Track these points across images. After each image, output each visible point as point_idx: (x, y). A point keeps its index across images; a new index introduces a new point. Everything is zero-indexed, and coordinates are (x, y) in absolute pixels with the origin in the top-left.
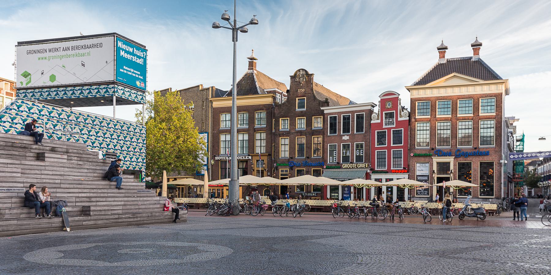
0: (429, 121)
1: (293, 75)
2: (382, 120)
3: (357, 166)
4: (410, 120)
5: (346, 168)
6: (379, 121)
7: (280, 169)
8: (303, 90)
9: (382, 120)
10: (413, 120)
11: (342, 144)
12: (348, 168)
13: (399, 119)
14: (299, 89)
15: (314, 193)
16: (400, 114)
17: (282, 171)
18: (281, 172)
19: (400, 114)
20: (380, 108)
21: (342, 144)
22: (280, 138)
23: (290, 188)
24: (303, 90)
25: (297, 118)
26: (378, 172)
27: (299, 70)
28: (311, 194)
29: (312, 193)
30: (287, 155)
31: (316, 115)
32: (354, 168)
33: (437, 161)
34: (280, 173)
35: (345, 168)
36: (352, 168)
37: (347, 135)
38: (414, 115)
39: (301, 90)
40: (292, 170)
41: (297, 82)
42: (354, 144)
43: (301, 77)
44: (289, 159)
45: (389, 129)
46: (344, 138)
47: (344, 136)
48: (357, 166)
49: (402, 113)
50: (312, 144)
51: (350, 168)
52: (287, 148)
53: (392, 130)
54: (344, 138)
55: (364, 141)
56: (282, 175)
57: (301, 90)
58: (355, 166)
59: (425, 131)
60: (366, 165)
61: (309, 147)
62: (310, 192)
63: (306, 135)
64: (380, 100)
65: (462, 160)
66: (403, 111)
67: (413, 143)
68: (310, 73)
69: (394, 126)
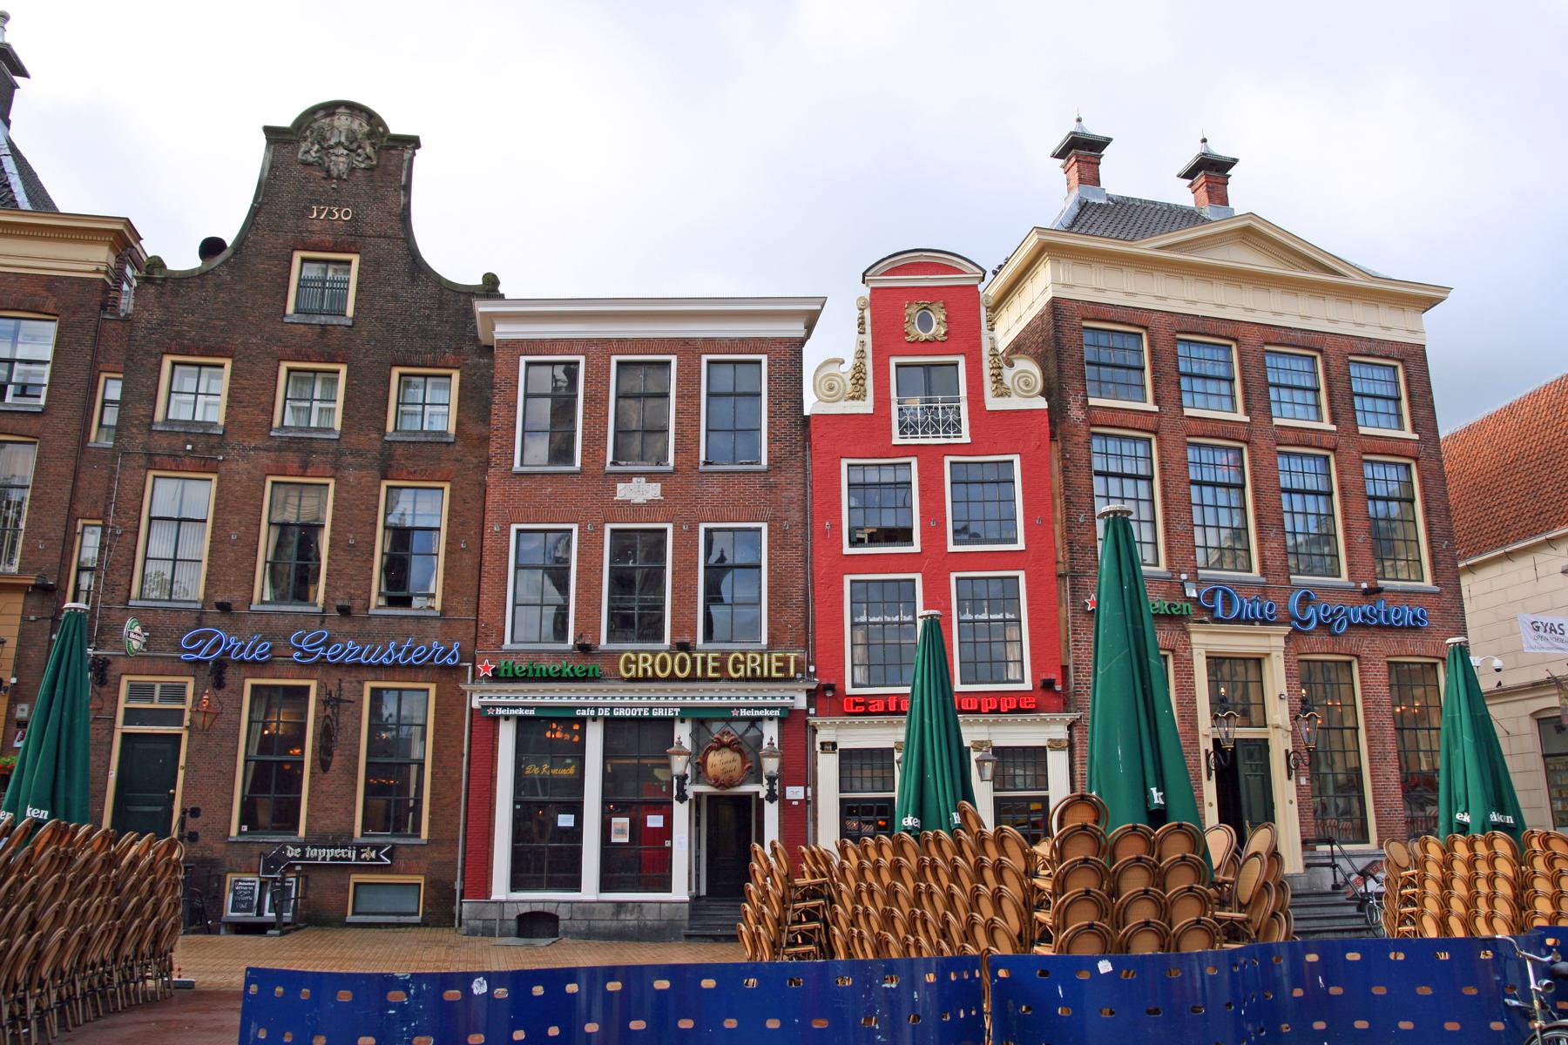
0: (1151, 427)
1: (286, 122)
2: (882, 401)
3: (721, 669)
4: (1057, 412)
5: (645, 679)
6: (866, 406)
7: (125, 680)
8: (342, 215)
9: (882, 401)
10: (1076, 413)
11: (608, 527)
12: (655, 679)
13: (992, 403)
14: (319, 203)
15: (374, 847)
16: (998, 379)
17: (138, 691)
18: (130, 697)
19: (998, 379)
20: (868, 338)
21: (608, 527)
22: (151, 474)
23: (195, 812)
24: (342, 215)
25: (284, 367)
26: (864, 708)
27: (331, 108)
28: (352, 854)
29: (359, 848)
30: (193, 586)
31: (416, 359)
32: (706, 679)
33: (1211, 648)
34: (122, 705)
35: (631, 680)
36: (692, 678)
37: (650, 477)
38: (1077, 384)
39: (331, 213)
40: (219, 684)
41: (306, 164)
42: (694, 531)
43: (339, 144)
44: (200, 618)
45: (930, 457)
46: (623, 491)
47: (627, 477)
48: (721, 669)
49: (1008, 374)
50: (375, 524)
51: (672, 678)
52: (198, 544)
53: (948, 460)
54: (623, 491)
55: (769, 512)
56: (132, 716)
57: (331, 213)
58: (710, 664)
59: (1128, 483)
60: (786, 661)
61: (352, 548)
62: (341, 839)
63: (336, 470)
64: (866, 292)
65: (1320, 650)
66: (1011, 365)
67: (1084, 539)
68: (397, 126)
69: (966, 438)
